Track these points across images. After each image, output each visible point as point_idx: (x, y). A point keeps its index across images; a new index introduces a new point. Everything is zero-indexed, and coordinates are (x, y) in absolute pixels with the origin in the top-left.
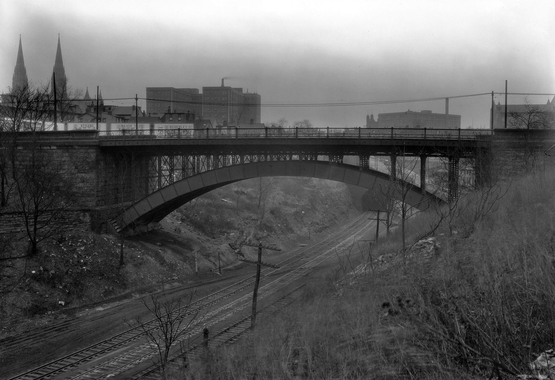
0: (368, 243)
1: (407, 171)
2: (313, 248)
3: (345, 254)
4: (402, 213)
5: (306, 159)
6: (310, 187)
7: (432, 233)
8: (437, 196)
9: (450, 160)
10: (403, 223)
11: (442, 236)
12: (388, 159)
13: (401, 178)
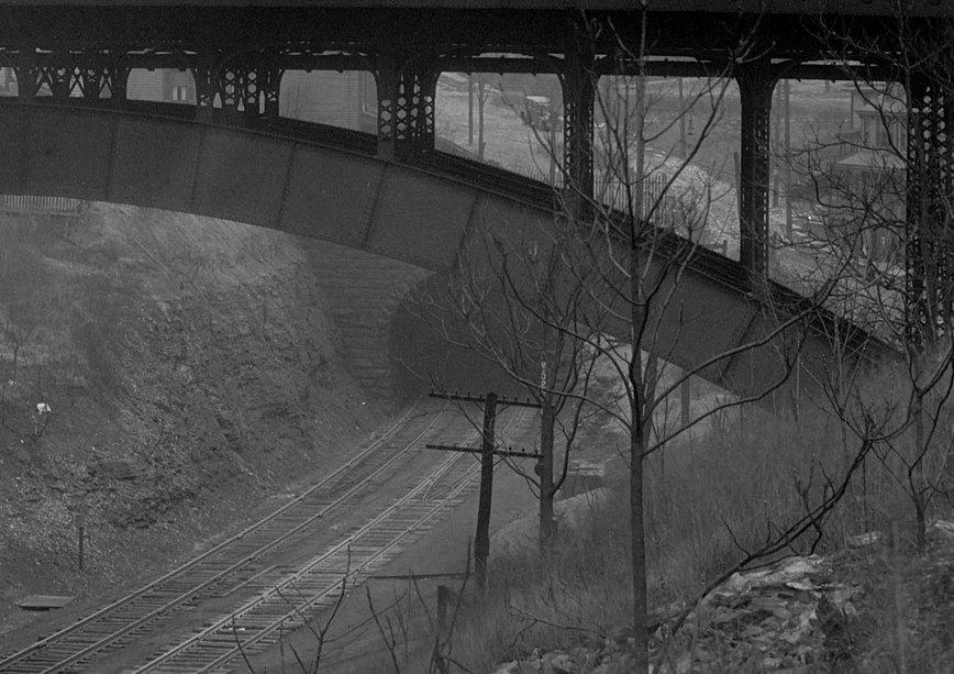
0: (429, 589)
1: (659, 164)
2: (103, 619)
3: (289, 656)
4: (628, 415)
5: (61, 89)
6: (84, 258)
7: (808, 532)
8: (838, 308)
9: (916, 98)
10: (637, 472)
11: (871, 549)
12: (544, 92)
13: (621, 203)
